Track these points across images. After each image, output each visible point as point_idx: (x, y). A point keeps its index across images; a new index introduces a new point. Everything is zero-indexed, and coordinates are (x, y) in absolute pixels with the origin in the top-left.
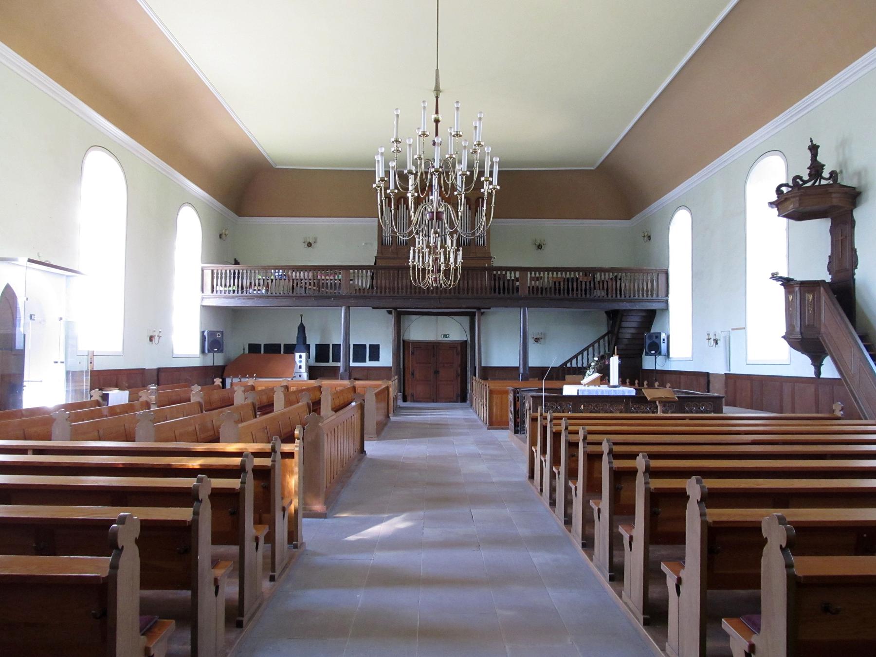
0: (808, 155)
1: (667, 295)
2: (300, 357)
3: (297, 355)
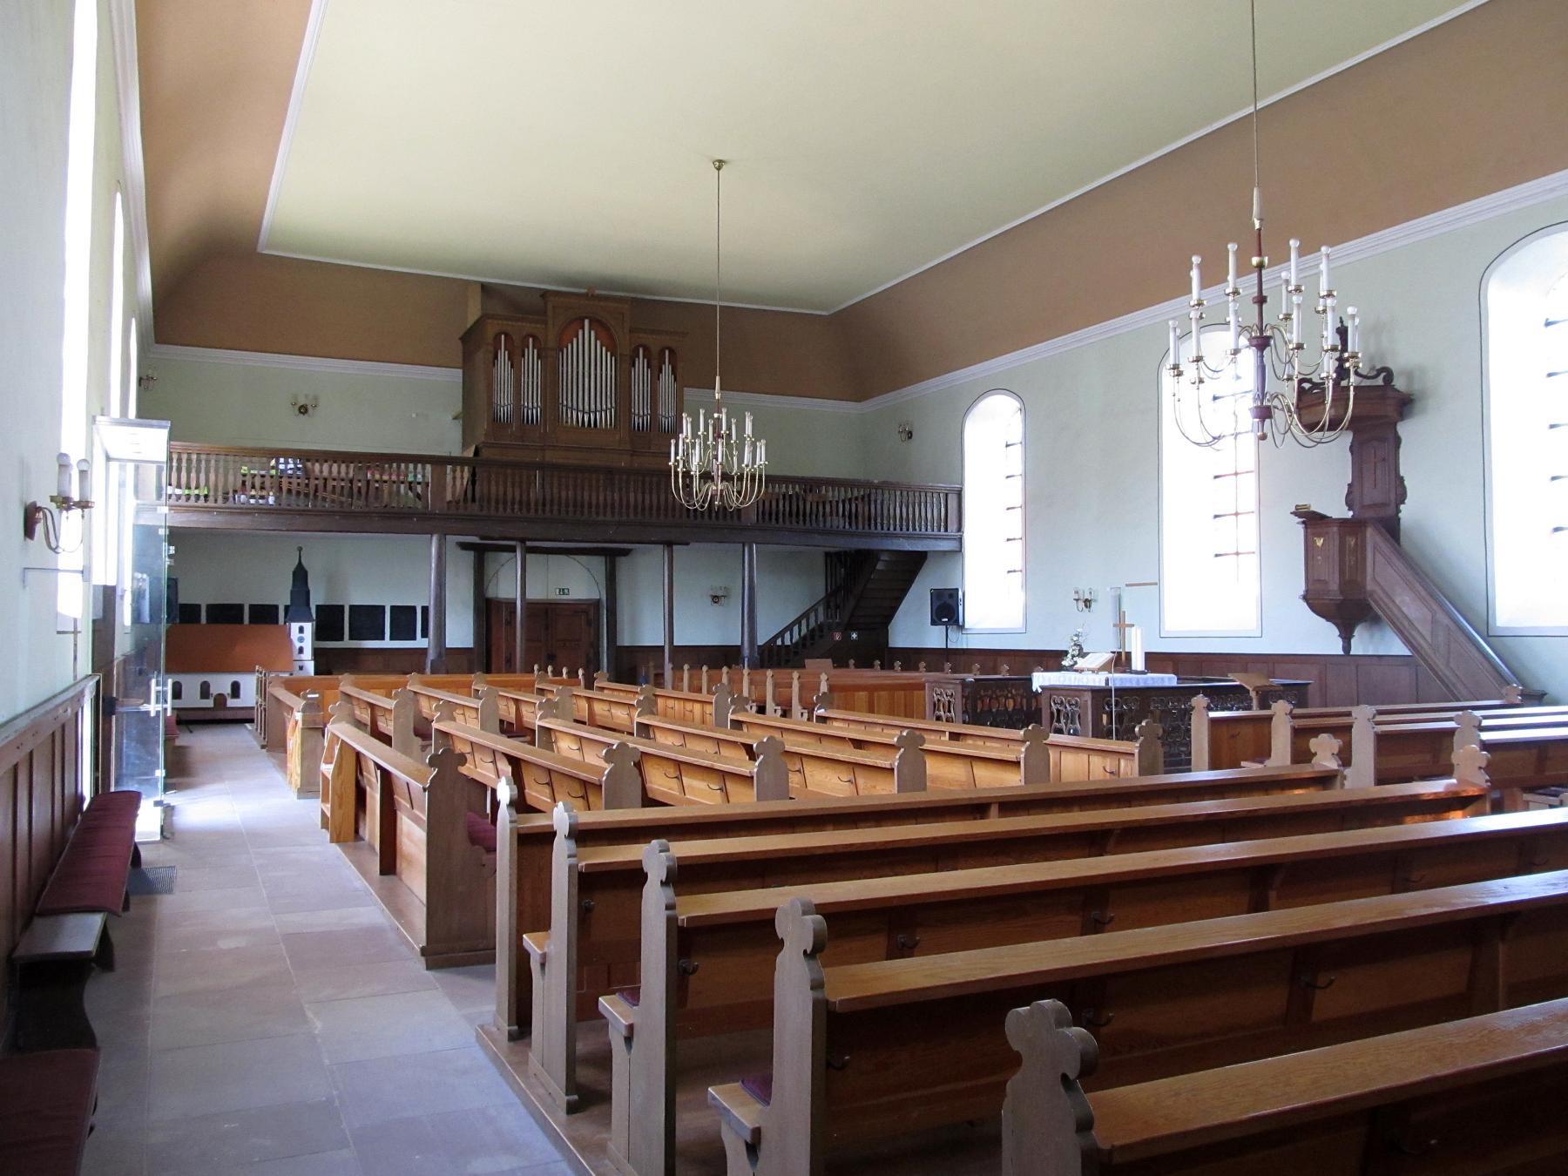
1: (960, 529)
2: (301, 630)
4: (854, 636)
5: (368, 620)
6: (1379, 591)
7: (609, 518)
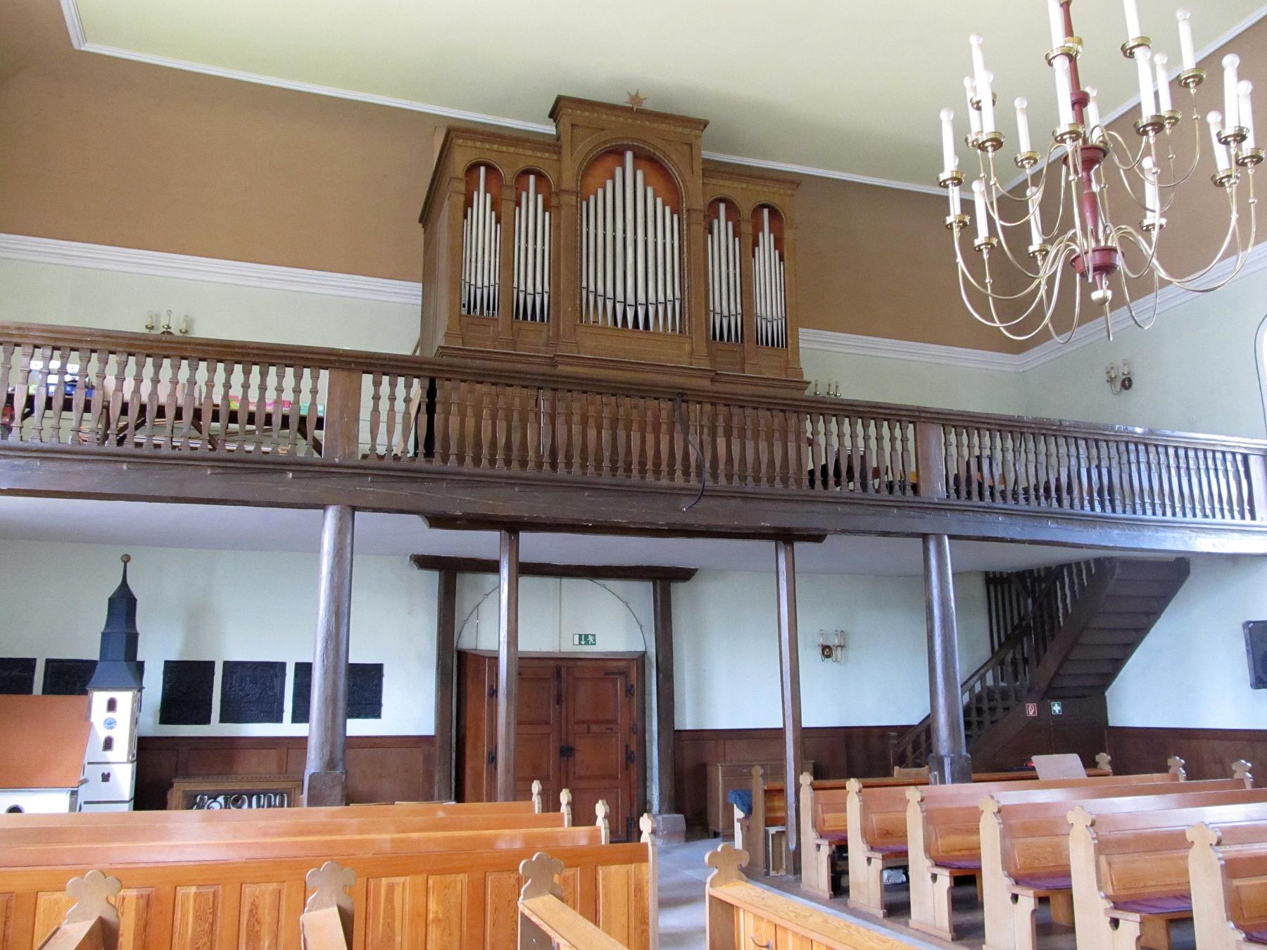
2: (112, 705)
3: (99, 699)
4: (1056, 708)
5: (256, 687)
7: (679, 480)
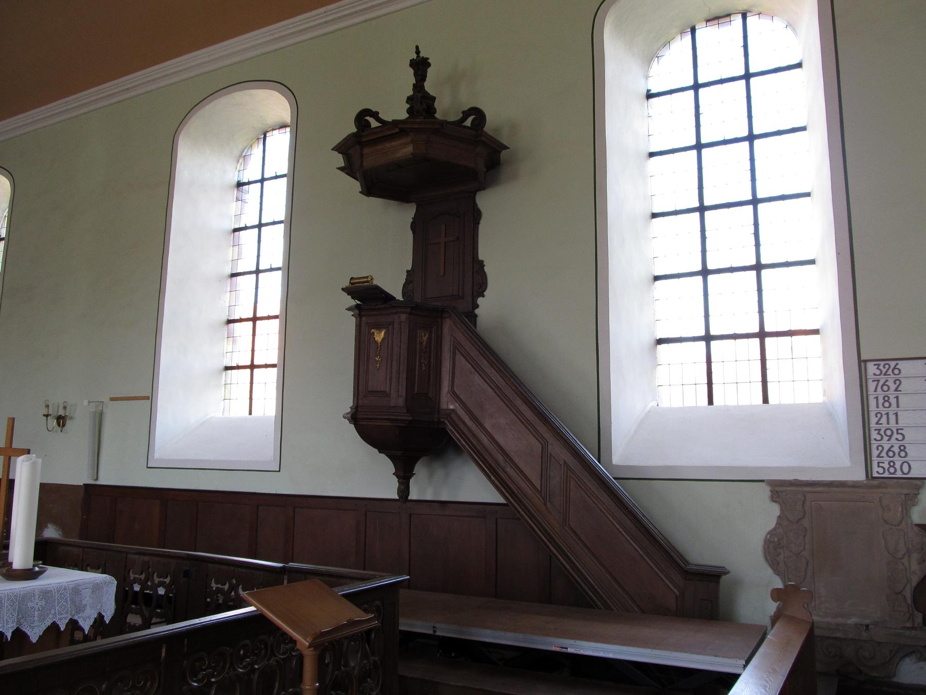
0: (409, 78)
6: (461, 413)
